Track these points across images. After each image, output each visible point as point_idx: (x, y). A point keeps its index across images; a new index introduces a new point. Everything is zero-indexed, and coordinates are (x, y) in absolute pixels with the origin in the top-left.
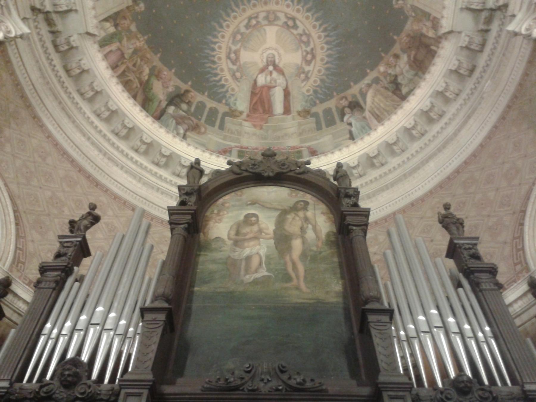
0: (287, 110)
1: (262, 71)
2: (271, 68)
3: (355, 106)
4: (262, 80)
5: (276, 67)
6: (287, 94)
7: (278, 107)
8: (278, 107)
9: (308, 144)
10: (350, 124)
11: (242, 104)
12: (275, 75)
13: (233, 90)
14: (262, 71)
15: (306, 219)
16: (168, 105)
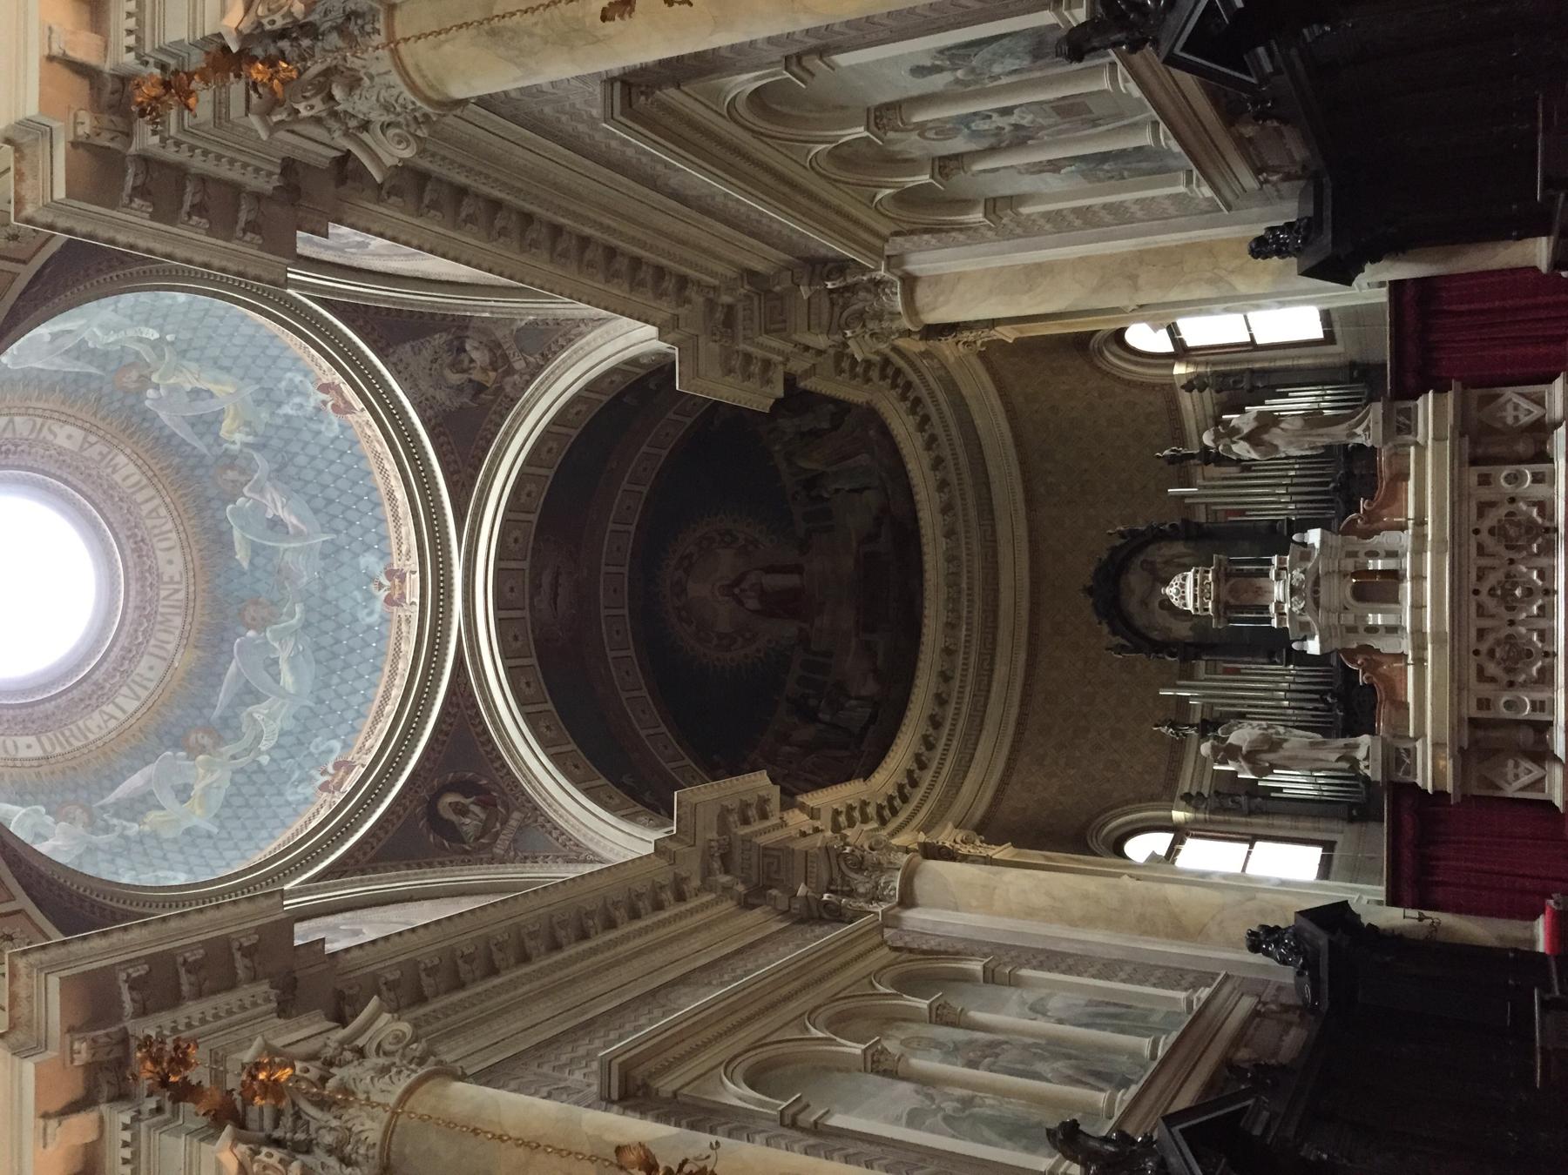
0: (797, 569)
1: (740, 603)
2: (736, 591)
3: (812, 482)
4: (752, 604)
5: (737, 582)
6: (771, 570)
7: (792, 580)
8: (792, 580)
9: (854, 544)
10: (837, 491)
11: (789, 629)
12: (745, 585)
13: (769, 641)
14: (740, 603)
15: (1166, 563)
16: (820, 721)
